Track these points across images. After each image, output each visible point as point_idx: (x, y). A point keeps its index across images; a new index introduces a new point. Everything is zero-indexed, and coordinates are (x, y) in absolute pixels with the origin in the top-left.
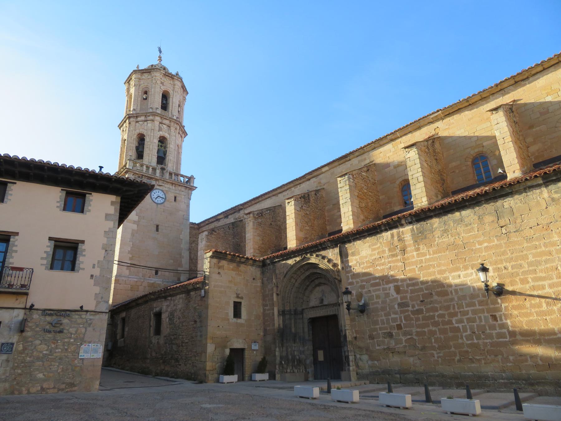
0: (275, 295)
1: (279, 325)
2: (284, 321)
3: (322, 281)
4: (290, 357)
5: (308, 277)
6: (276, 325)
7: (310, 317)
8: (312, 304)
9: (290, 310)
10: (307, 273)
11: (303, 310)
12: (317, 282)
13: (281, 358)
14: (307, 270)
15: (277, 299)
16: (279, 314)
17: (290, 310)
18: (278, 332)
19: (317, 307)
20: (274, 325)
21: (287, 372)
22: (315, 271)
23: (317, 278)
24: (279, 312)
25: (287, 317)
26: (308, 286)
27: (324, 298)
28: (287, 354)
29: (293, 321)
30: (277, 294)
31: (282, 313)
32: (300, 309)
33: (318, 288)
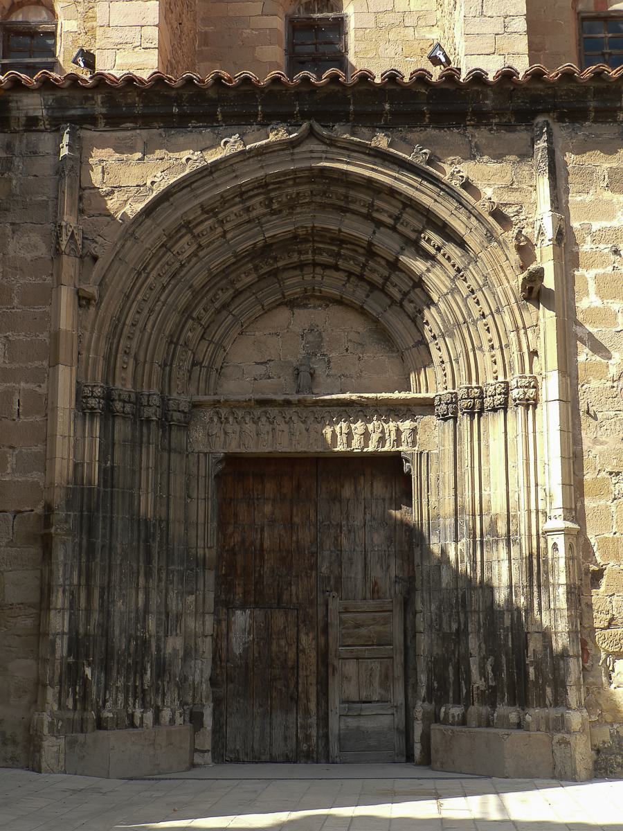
0: (66, 297)
1: (76, 465)
2: (107, 448)
3: (332, 283)
4: (120, 642)
5: (265, 251)
6: (62, 468)
7: (233, 448)
8: (236, 387)
9: (139, 396)
10: (278, 229)
11: (195, 405)
12: (294, 283)
13: (77, 645)
14: (274, 213)
15: (79, 324)
16: (83, 409)
17: (139, 396)
18: (69, 505)
19: (287, 403)
20: (45, 461)
21: (100, 724)
22: (330, 222)
23: (301, 266)
24: (81, 396)
25: (122, 430)
26: (238, 293)
27: (320, 368)
28: (106, 630)
29: (148, 457)
30: (83, 300)
31: (99, 407)
32: (180, 399)
33: (283, 315)
